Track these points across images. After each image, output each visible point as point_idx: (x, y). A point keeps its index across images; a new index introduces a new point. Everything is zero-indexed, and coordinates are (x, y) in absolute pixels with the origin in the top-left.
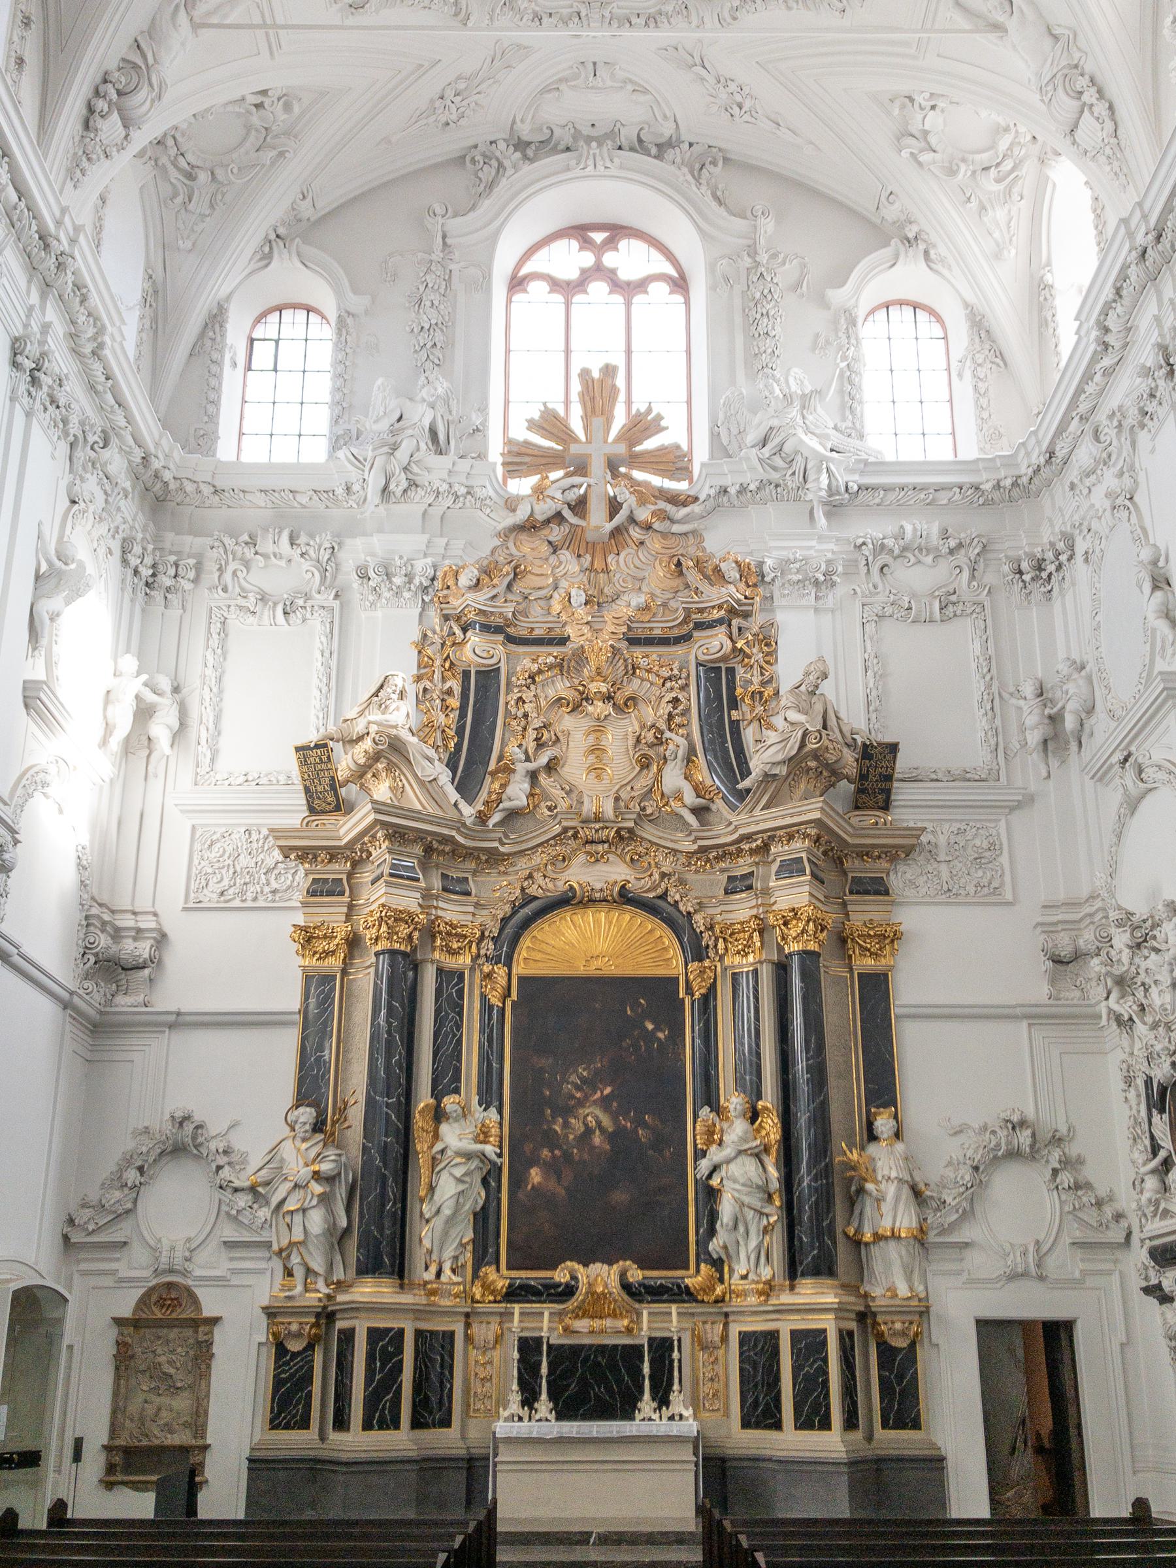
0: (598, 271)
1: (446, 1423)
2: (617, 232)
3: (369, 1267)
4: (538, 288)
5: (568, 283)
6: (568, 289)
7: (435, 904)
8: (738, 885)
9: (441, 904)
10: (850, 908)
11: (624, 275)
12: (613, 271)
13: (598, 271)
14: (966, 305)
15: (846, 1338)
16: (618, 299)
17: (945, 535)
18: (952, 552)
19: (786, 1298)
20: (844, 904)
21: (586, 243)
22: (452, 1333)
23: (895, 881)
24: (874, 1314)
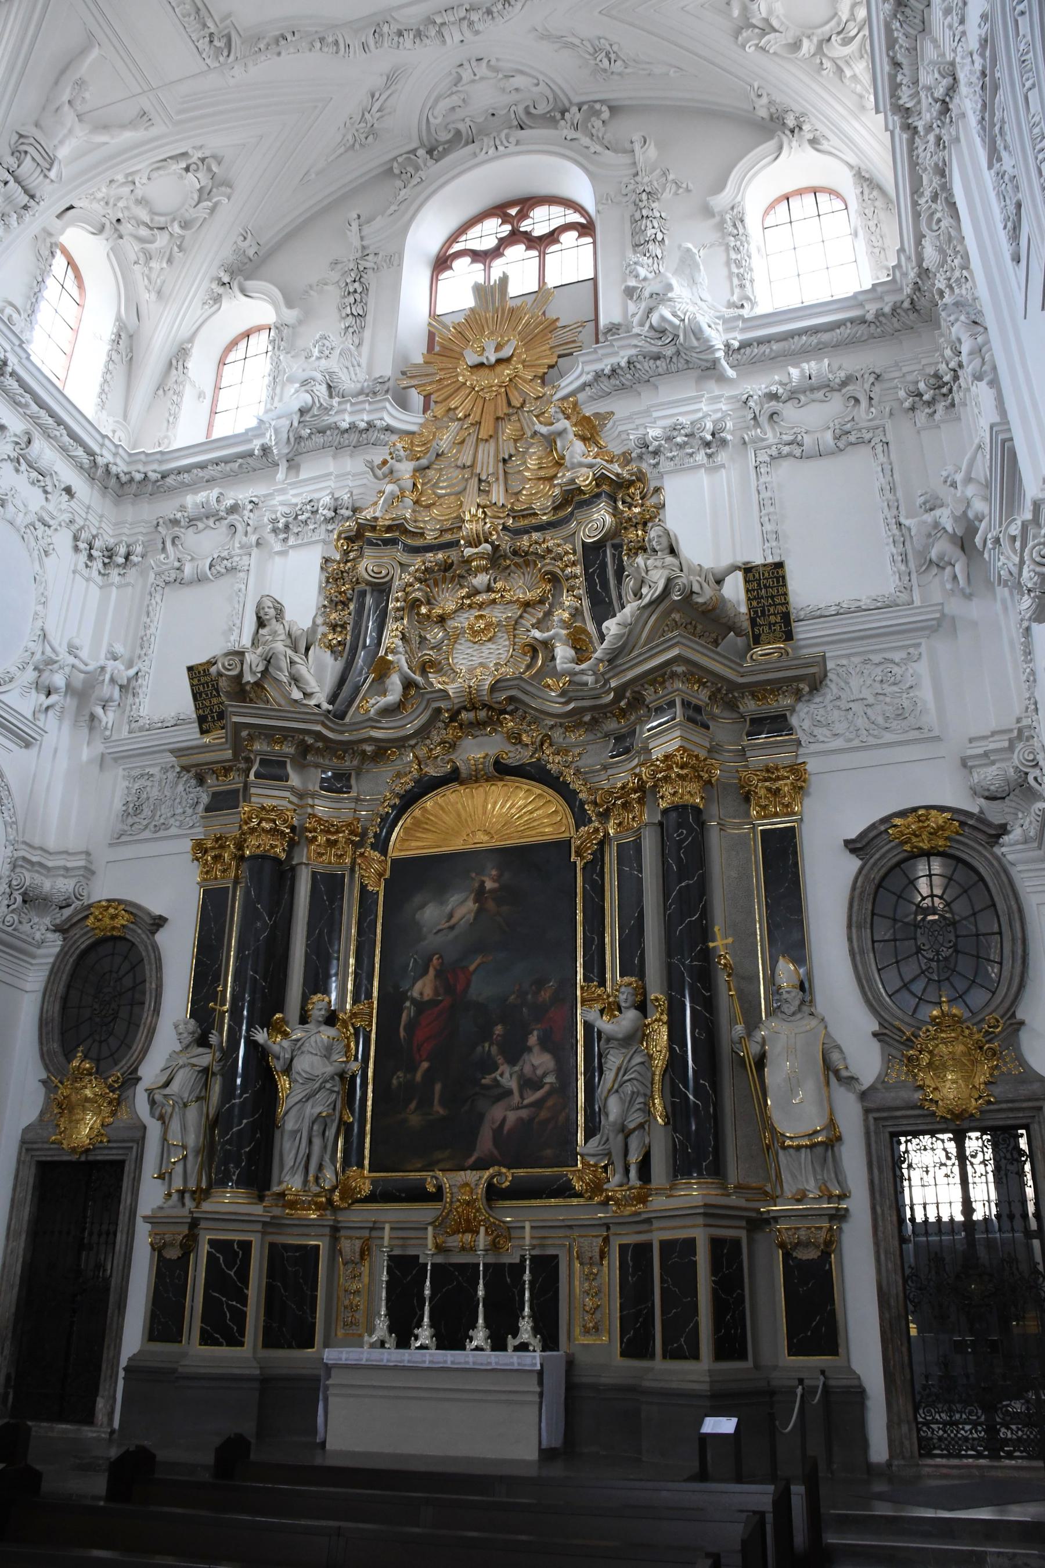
7: (310, 801)
10: (748, 754)
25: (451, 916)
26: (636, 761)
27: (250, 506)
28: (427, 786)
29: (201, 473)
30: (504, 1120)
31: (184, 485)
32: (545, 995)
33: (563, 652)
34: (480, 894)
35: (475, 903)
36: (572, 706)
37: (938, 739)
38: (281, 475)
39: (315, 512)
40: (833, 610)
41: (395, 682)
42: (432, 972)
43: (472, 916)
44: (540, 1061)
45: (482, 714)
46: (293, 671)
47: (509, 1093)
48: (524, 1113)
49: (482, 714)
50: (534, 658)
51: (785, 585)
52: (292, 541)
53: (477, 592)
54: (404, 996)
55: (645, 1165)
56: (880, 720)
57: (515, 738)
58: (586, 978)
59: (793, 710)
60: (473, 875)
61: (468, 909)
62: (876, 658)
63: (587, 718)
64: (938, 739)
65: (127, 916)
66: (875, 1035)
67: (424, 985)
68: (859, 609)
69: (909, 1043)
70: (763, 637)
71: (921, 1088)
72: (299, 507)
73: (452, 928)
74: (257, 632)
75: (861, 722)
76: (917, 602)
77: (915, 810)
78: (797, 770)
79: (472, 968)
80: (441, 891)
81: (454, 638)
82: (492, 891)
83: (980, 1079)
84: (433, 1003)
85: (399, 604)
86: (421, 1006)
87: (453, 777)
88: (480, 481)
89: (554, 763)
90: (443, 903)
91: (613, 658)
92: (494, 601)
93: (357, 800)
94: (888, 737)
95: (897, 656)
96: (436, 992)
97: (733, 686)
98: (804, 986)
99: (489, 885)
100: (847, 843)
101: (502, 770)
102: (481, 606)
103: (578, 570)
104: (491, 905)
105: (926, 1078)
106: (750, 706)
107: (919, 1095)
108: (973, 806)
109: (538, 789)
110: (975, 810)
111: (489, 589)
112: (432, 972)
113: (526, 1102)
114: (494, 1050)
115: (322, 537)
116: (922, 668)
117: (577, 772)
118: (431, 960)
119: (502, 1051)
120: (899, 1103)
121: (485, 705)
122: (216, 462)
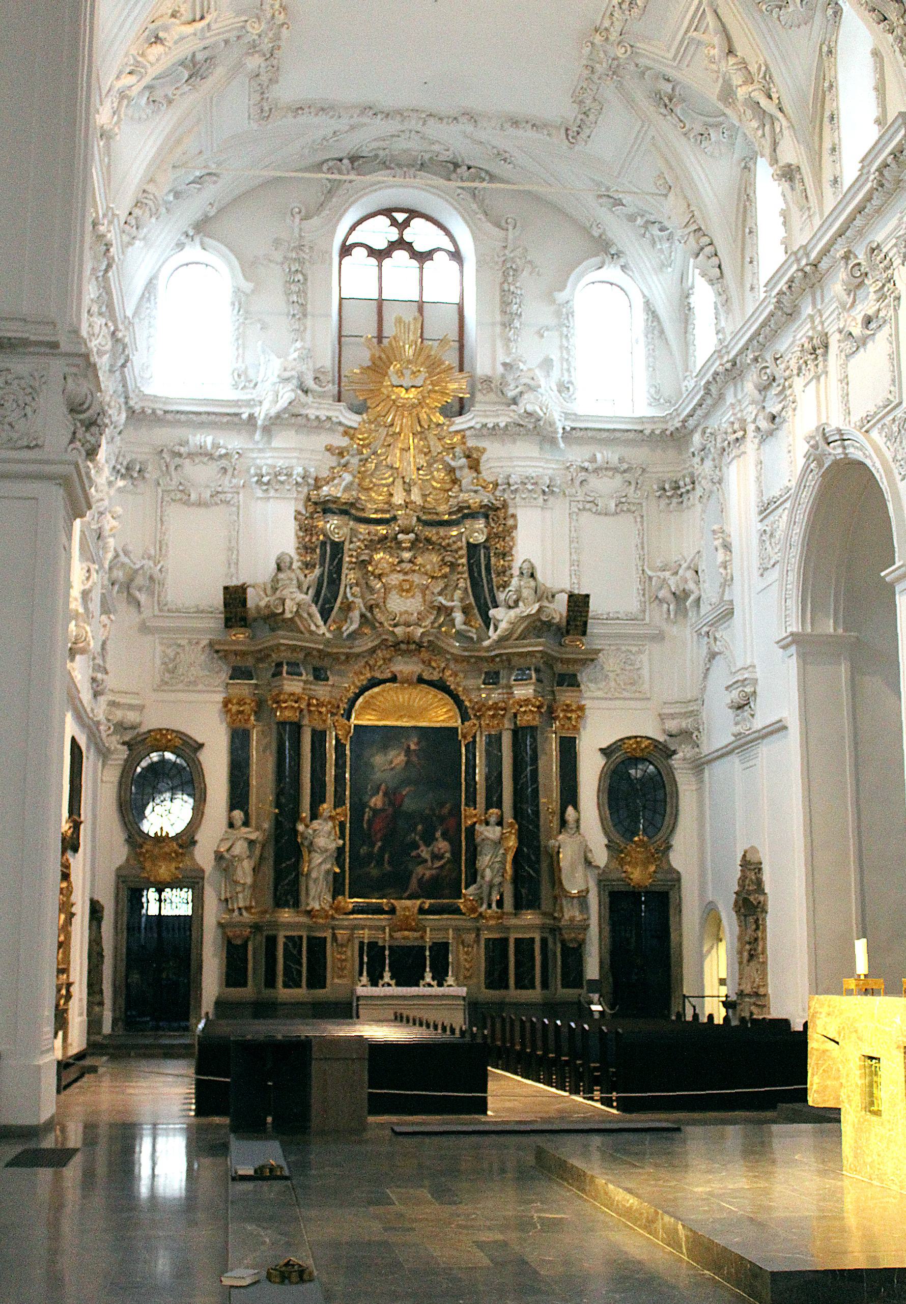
0: (401, 244)
1: (324, 987)
2: (413, 214)
3: (279, 903)
4: (359, 253)
5: (380, 251)
6: (380, 255)
8: (492, 679)
9: (313, 687)
11: (419, 247)
12: (410, 244)
13: (401, 244)
14: (644, 296)
15: (544, 941)
16: (414, 263)
17: (621, 460)
18: (625, 471)
19: (514, 921)
20: (553, 692)
21: (394, 223)
22: (325, 938)
23: (582, 677)
24: (560, 929)
25: (391, 762)
26: (500, 691)
27: (237, 456)
28: (374, 683)
29: (194, 417)
30: (424, 874)
31: (179, 421)
32: (445, 811)
33: (459, 617)
34: (408, 751)
35: (405, 756)
36: (466, 654)
37: (649, 699)
38: (257, 436)
39: (289, 475)
40: (605, 617)
41: (355, 615)
42: (381, 794)
43: (403, 764)
44: (442, 845)
45: (413, 647)
46: (311, 611)
47: (426, 861)
48: (434, 872)
49: (413, 647)
50: (438, 615)
51: (588, 607)
52: (272, 493)
53: (401, 561)
54: (364, 805)
55: (500, 904)
56: (622, 684)
57: (427, 663)
58: (466, 805)
59: (578, 671)
60: (403, 740)
61: (401, 758)
62: (623, 648)
63: (473, 660)
64: (649, 699)
65: (177, 739)
66: (606, 846)
67: (377, 800)
68: (618, 618)
69: (622, 852)
70: (571, 632)
71: (625, 872)
72: (278, 469)
73: (392, 769)
74: (276, 575)
75: (613, 684)
76: (647, 621)
77: (636, 737)
78: (581, 708)
79: (404, 793)
80: (385, 748)
81: (387, 589)
82: (415, 750)
83: (652, 868)
84: (382, 810)
85: (354, 560)
86: (375, 811)
87: (393, 679)
88: (404, 482)
89: (451, 682)
90: (385, 755)
91: (502, 639)
92: (414, 571)
93: (333, 685)
94: (625, 694)
95: (634, 649)
96: (384, 804)
97: (554, 658)
98: (578, 821)
99: (413, 747)
100: (601, 750)
101: (421, 680)
102: (406, 573)
103: (464, 561)
104: (414, 759)
105: (627, 868)
106: (559, 668)
107: (624, 875)
108: (661, 738)
109: (441, 695)
110: (661, 740)
111: (410, 561)
112: (381, 794)
113: (435, 866)
114: (417, 838)
115: (295, 496)
116: (644, 657)
117: (464, 689)
118: (380, 785)
119: (422, 838)
120: (615, 878)
121: (414, 642)
122: (208, 413)
